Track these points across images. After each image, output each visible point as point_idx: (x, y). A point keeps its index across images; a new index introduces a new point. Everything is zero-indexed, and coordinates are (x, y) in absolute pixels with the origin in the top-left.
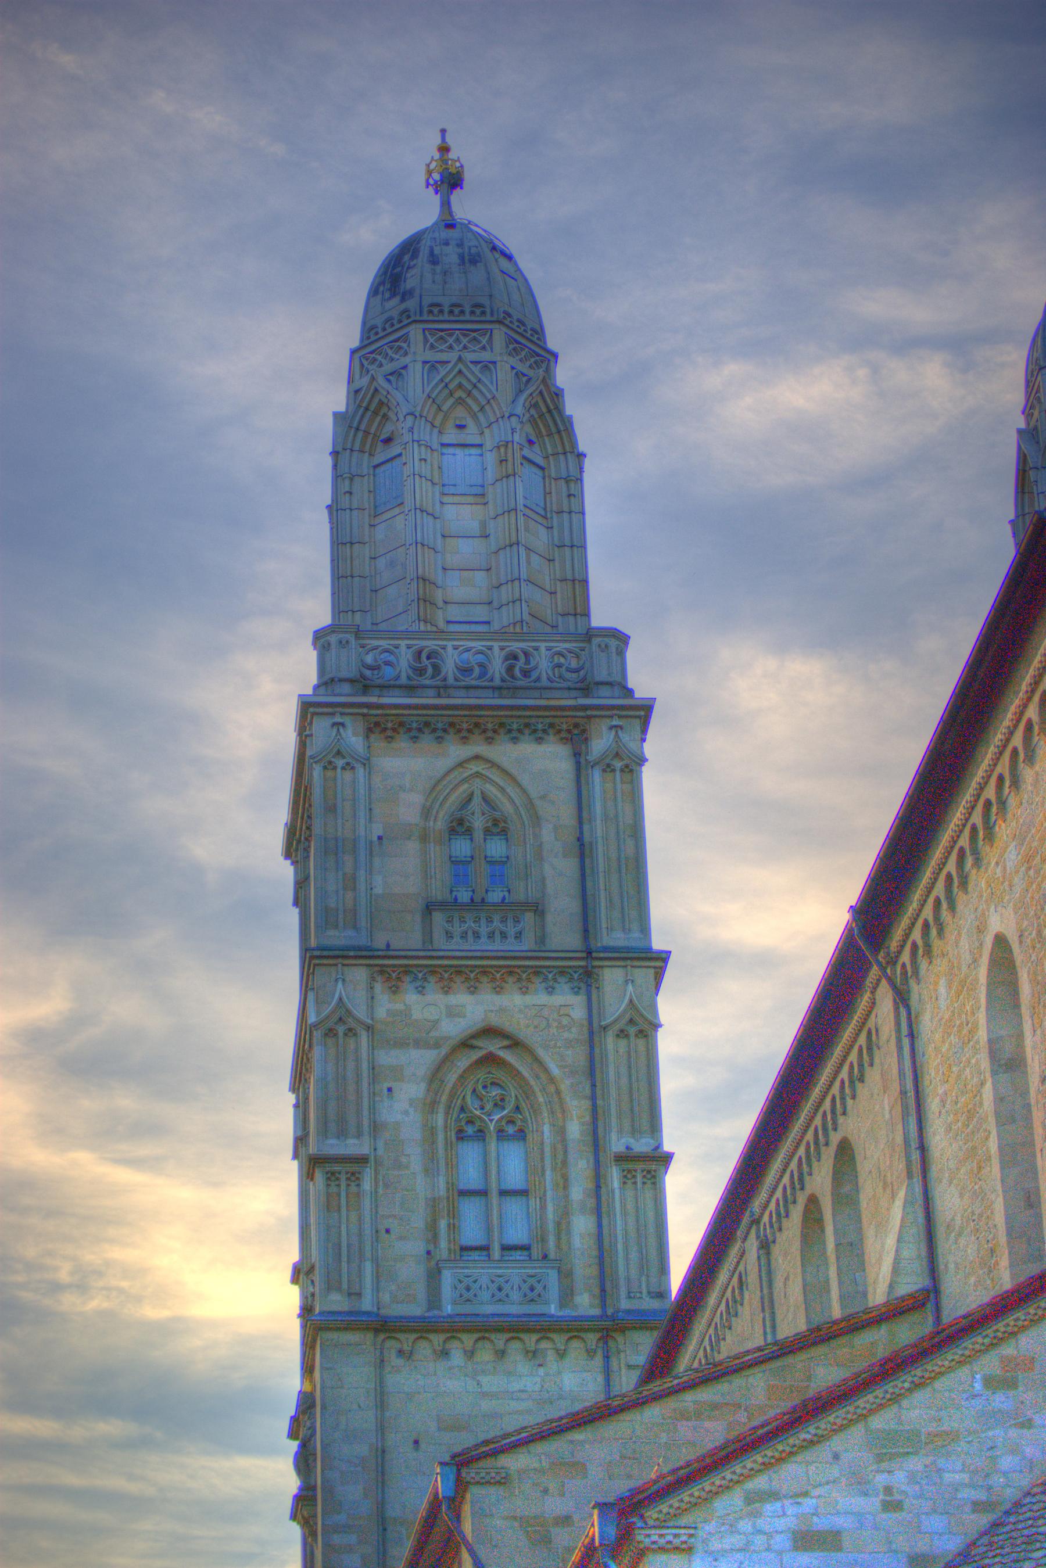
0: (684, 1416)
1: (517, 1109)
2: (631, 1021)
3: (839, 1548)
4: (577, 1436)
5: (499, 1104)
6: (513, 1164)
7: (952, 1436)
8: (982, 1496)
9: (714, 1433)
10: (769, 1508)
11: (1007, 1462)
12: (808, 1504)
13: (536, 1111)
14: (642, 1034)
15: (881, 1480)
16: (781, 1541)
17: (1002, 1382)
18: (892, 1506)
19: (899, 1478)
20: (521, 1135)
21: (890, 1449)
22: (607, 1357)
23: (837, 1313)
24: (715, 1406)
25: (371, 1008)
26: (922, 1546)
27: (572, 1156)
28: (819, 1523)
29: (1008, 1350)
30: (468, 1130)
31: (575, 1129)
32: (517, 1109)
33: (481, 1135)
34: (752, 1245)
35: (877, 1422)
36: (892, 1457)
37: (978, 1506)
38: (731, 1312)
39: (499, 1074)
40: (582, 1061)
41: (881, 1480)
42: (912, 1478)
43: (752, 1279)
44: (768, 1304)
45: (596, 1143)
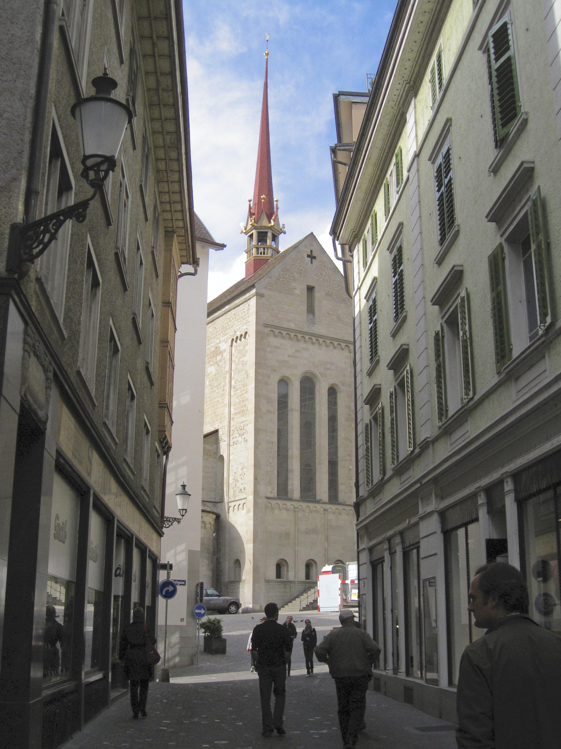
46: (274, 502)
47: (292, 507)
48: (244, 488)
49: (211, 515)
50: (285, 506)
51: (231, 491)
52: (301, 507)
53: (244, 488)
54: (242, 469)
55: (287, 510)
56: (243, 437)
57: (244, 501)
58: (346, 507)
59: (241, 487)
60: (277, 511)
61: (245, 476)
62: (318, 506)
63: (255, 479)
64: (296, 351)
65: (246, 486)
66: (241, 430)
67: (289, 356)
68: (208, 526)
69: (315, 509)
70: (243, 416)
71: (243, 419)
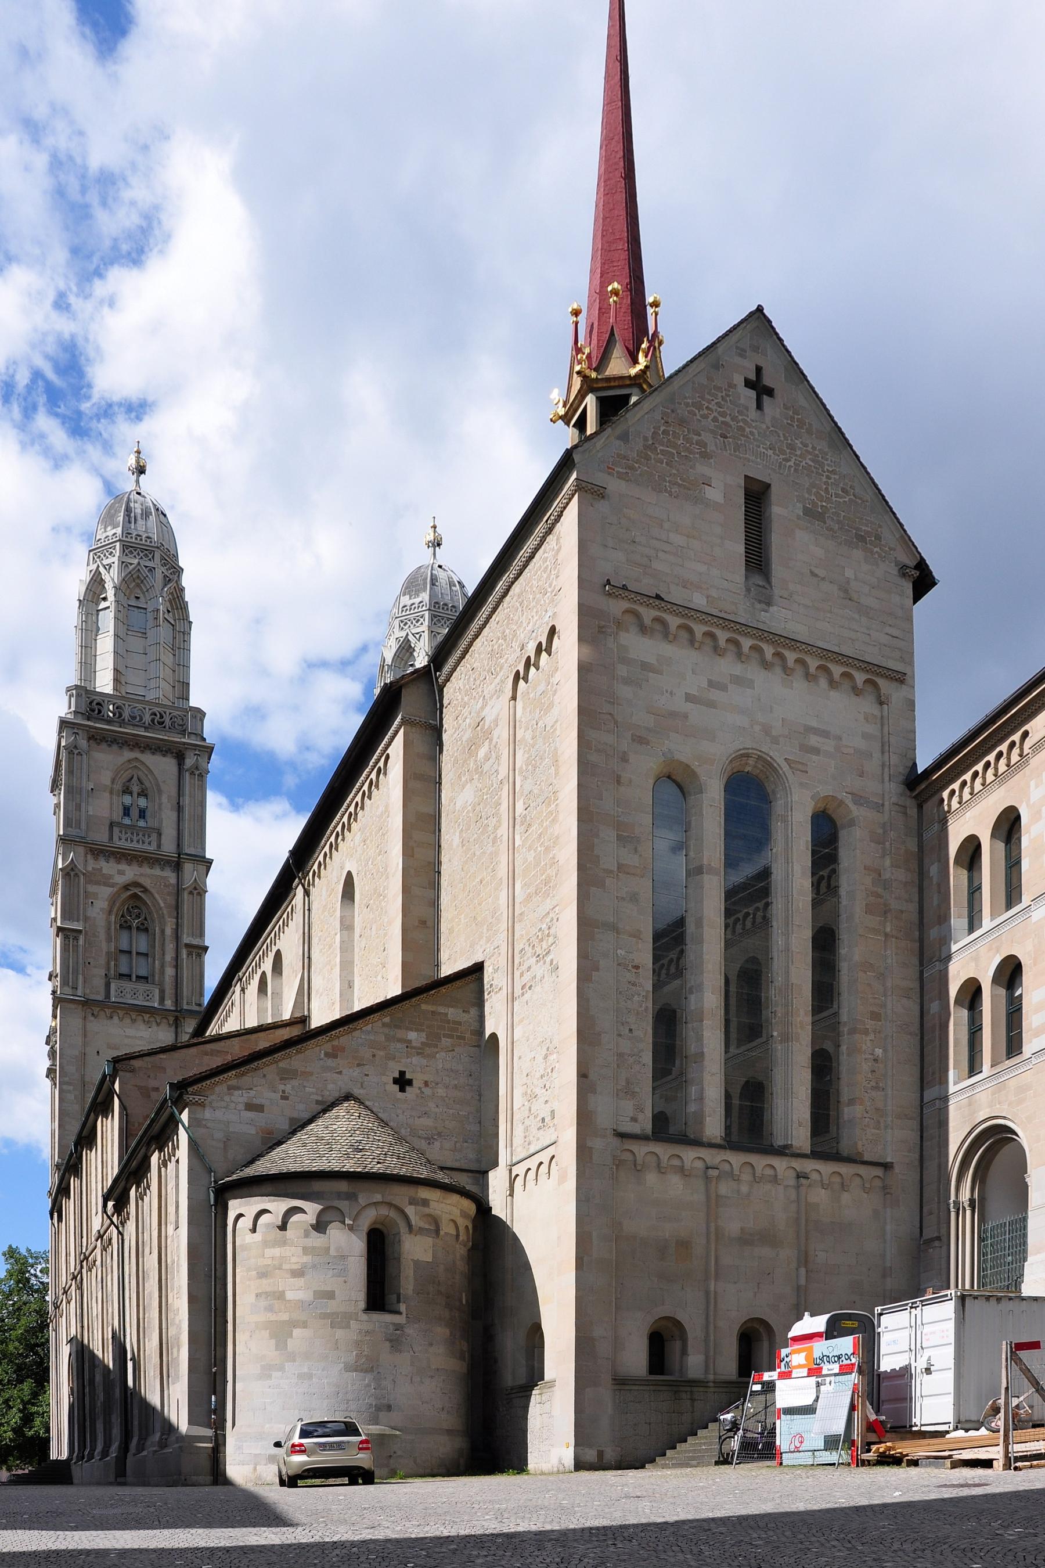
0: (206, 1054)
1: (146, 919)
2: (195, 889)
3: (263, 1112)
4: (162, 1056)
5: (138, 916)
6: (141, 943)
7: (311, 1074)
8: (320, 1098)
9: (217, 1062)
10: (236, 1093)
11: (330, 1086)
12: (252, 1093)
13: (153, 921)
14: (199, 894)
15: (282, 1087)
16: (241, 1107)
17: (332, 1055)
18: (285, 1098)
19: (288, 1088)
20: (146, 930)
21: (286, 1075)
22: (176, 1028)
23: (270, 1021)
24: (218, 1052)
25: (85, 865)
26: (295, 1115)
27: (167, 941)
28: (255, 1101)
29: (335, 1043)
30: (125, 926)
31: (168, 931)
32: (146, 919)
33: (130, 928)
34: (238, 988)
35: (281, 1065)
36: (286, 1079)
37: (318, 1102)
38: (227, 1016)
39: (138, 904)
40: (174, 903)
41: (282, 1087)
42: (293, 1087)
43: (237, 1003)
44: (242, 1013)
45: (177, 937)
46: (641, 1150)
47: (699, 1164)
48: (553, 1112)
49: (455, 1198)
50: (676, 1162)
51: (519, 1131)
52: (727, 1167)
53: (553, 1112)
54: (546, 1057)
55: (681, 1170)
56: (548, 959)
57: (550, 1151)
58: (862, 1170)
59: (545, 1113)
60: (651, 1178)
61: (555, 1075)
62: (780, 1164)
63: (583, 1075)
64: (711, 684)
65: (555, 1105)
66: (542, 940)
67: (689, 698)
68: (447, 1229)
69: (769, 1172)
70: (547, 895)
71: (548, 904)
